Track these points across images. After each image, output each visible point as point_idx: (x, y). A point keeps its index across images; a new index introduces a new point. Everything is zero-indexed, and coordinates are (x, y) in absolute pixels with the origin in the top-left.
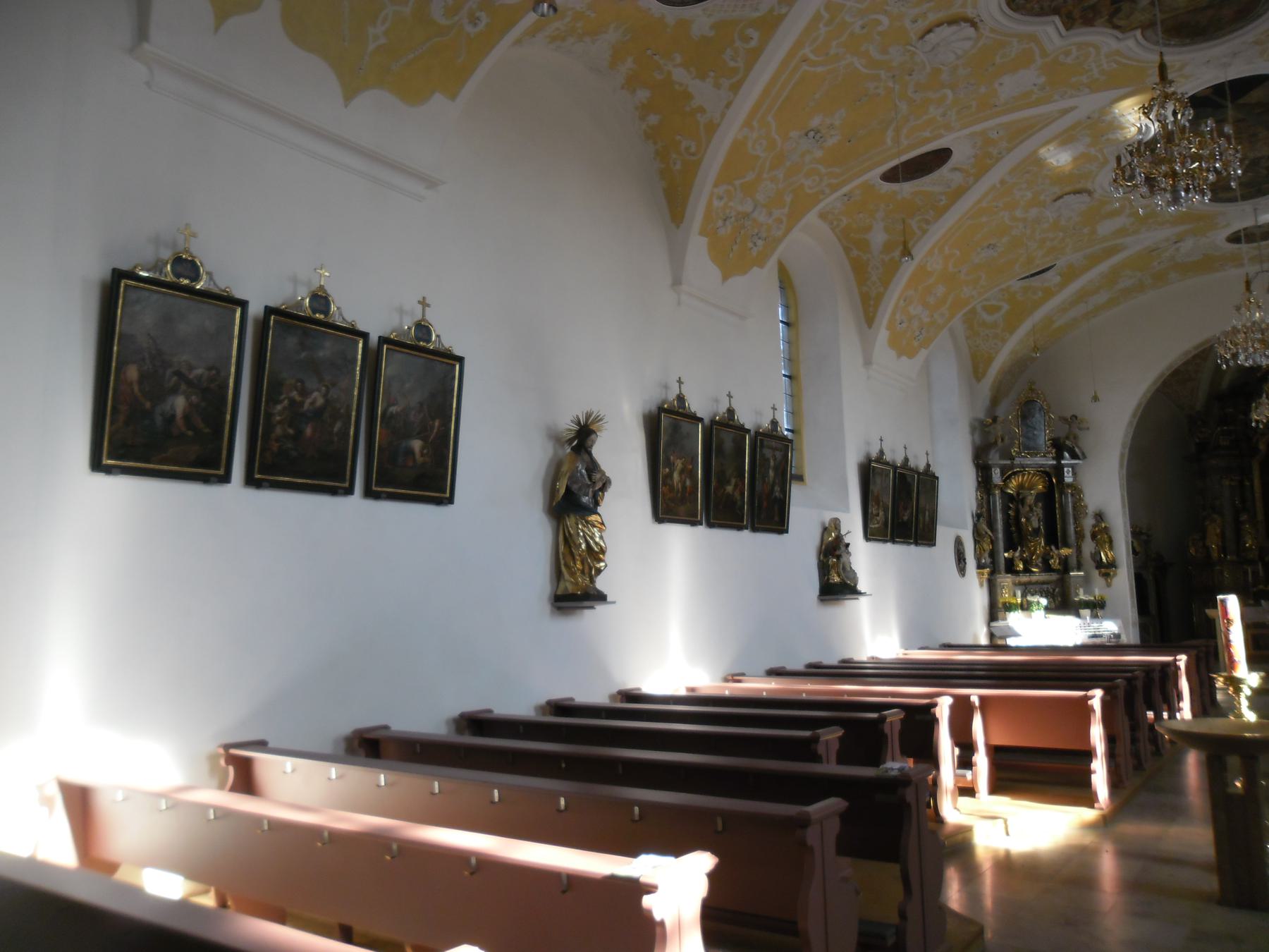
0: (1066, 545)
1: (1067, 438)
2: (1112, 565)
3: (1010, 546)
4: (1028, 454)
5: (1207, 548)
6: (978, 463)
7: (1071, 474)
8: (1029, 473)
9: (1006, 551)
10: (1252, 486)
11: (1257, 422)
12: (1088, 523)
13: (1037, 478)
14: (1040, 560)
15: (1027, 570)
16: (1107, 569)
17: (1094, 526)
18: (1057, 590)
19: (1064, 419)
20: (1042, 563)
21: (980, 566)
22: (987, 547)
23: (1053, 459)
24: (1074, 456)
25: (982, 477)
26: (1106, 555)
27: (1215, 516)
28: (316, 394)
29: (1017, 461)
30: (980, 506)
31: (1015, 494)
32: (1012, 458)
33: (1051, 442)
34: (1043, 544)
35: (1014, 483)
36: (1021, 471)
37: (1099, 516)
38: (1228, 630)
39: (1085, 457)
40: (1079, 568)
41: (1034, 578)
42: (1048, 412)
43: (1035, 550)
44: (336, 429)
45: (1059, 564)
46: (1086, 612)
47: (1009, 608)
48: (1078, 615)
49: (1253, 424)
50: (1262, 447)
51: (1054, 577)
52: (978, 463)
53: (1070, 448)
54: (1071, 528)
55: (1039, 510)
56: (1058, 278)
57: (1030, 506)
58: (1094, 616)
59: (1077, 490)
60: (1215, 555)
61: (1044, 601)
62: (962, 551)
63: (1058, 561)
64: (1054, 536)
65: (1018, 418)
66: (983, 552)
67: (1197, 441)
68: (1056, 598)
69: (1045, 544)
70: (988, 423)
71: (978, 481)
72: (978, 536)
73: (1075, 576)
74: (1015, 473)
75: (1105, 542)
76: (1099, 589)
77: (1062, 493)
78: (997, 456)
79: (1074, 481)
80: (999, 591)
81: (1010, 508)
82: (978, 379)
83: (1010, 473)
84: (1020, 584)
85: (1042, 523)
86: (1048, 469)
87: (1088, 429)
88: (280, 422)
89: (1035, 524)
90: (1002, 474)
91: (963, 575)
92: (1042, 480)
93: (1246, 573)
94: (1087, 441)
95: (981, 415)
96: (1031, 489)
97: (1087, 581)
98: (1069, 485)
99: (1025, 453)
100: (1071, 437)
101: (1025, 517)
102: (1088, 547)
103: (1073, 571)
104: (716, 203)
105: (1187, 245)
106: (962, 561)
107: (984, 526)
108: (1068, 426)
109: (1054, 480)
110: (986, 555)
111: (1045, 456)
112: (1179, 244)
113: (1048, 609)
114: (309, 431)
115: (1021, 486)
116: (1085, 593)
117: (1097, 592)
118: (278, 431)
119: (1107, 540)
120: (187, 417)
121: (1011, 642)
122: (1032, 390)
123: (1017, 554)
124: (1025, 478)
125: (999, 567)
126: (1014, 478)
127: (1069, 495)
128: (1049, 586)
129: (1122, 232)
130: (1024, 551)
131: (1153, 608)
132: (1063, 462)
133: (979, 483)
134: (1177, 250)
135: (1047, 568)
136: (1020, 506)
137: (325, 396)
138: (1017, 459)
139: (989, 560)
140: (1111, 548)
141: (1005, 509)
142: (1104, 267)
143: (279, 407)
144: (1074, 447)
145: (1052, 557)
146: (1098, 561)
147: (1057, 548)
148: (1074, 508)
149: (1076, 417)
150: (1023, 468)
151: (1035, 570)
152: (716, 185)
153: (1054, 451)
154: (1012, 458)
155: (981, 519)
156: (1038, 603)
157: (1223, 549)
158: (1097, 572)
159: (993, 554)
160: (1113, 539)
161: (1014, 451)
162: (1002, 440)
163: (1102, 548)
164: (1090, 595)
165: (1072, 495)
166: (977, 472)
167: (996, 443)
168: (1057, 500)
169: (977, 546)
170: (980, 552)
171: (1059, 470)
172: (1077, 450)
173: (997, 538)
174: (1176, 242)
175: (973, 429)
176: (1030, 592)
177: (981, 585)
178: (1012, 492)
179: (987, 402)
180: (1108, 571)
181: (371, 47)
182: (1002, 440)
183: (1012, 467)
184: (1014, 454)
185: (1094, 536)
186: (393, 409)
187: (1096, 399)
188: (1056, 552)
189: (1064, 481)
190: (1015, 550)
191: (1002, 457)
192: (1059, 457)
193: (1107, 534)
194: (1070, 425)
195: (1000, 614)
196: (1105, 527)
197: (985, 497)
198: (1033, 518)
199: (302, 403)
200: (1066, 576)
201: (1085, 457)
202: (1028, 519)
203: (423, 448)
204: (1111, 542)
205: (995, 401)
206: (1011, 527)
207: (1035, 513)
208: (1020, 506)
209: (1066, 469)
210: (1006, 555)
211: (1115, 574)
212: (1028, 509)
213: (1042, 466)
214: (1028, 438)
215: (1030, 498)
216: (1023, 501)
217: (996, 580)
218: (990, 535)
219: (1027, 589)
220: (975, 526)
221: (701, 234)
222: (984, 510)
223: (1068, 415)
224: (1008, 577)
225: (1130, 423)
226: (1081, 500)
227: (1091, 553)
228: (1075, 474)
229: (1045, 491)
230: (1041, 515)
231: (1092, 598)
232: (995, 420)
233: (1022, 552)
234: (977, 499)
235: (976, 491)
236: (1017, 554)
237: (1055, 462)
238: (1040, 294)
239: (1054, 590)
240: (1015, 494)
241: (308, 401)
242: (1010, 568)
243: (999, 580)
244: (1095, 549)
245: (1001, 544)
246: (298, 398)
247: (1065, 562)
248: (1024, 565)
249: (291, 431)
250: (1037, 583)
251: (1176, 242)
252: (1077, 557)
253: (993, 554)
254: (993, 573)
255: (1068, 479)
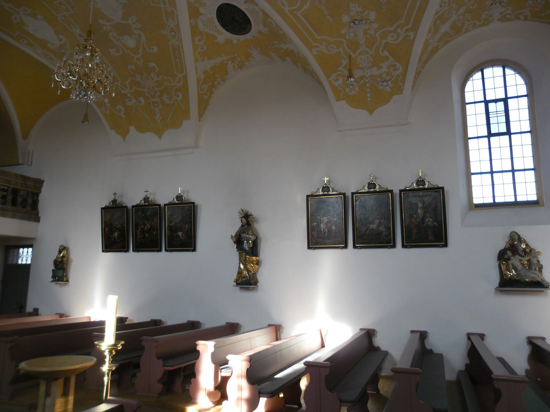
28: (148, 225)
44: (154, 233)
88: (139, 234)
104: (336, 84)
114: (147, 235)
118: (139, 237)
120: (118, 237)
137: (150, 225)
143: (139, 231)
152: (328, 77)
181: (159, 121)
186: (171, 224)
199: (144, 228)
203: (182, 235)
221: (338, 100)
241: (146, 227)
246: (143, 227)
249: (142, 236)
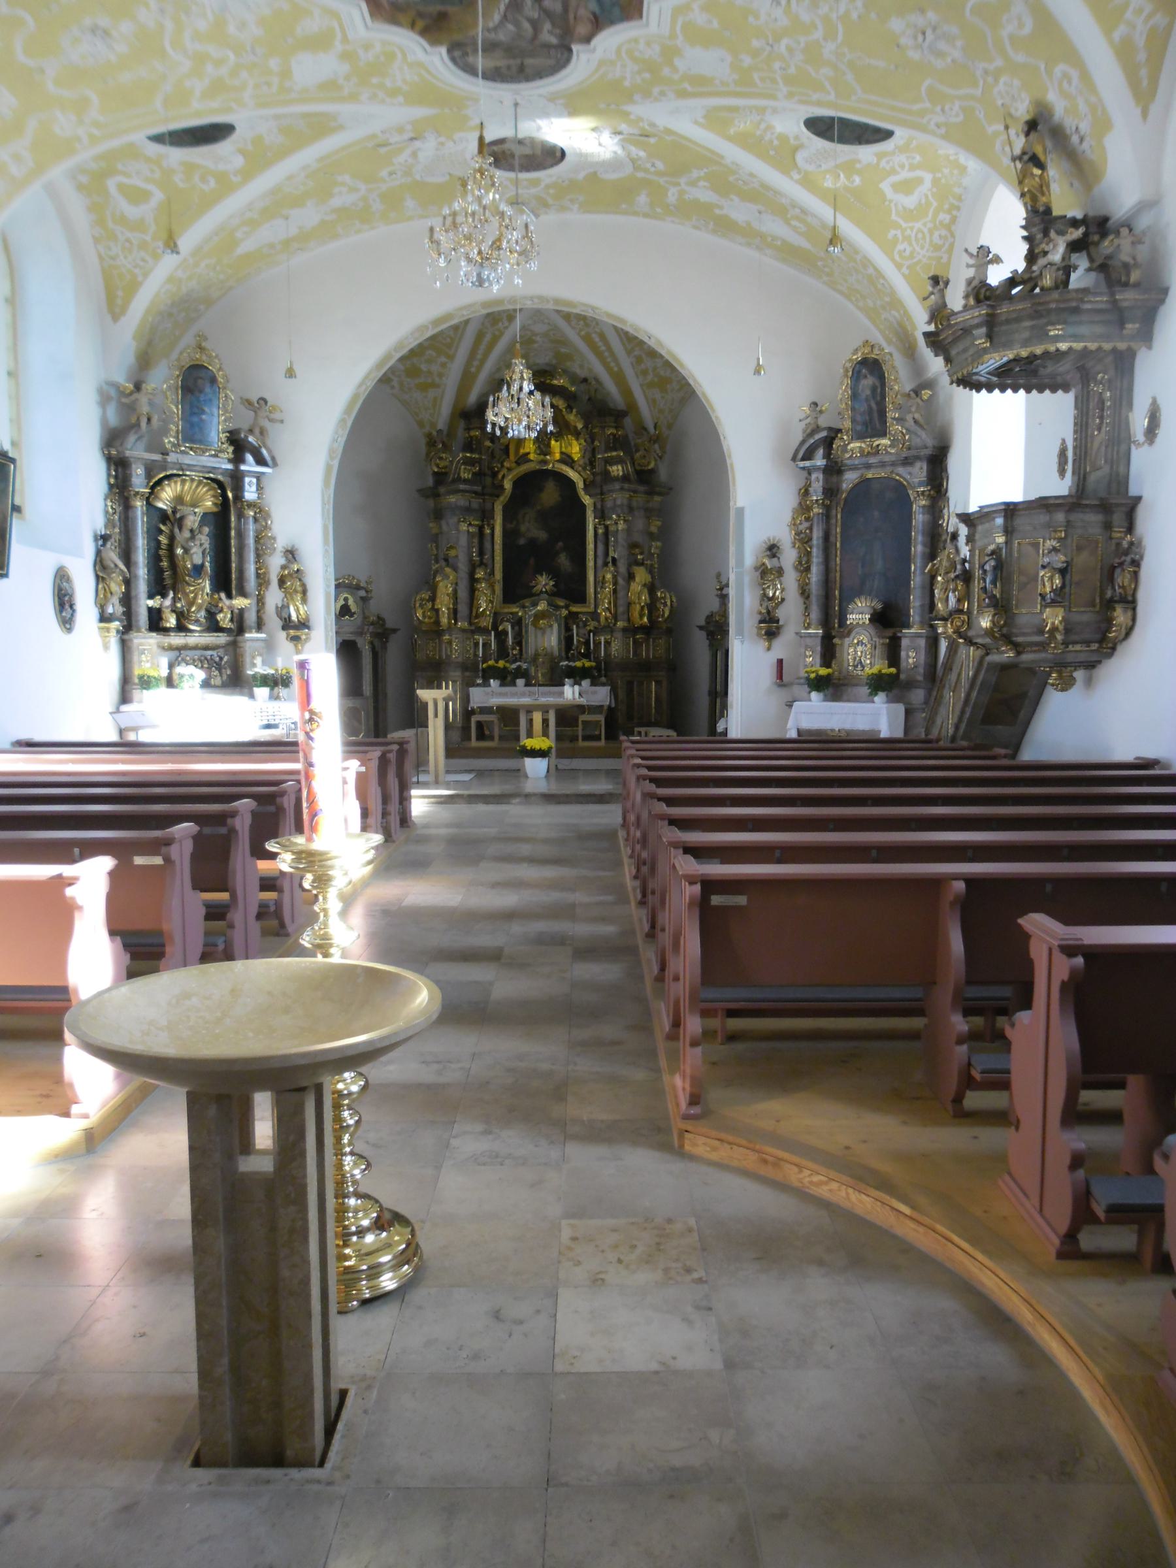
0: (243, 593)
1: (251, 431)
2: (304, 625)
3: (158, 588)
4: (191, 449)
5: (437, 611)
6: (109, 454)
7: (254, 488)
8: (192, 480)
9: (151, 597)
10: (493, 535)
11: (494, 425)
12: (275, 562)
13: (205, 489)
14: (203, 613)
15: (181, 628)
16: (296, 628)
17: (283, 567)
18: (226, 659)
19: (248, 403)
20: (205, 618)
21: (104, 618)
22: (118, 588)
23: (230, 461)
24: (261, 461)
25: (116, 477)
26: (297, 610)
27: (448, 570)
29: (172, 458)
30: (109, 523)
31: (170, 512)
32: (165, 453)
33: (228, 434)
34: (208, 589)
35: (167, 496)
36: (179, 475)
37: (291, 554)
38: (311, 739)
39: (275, 464)
40: (260, 626)
41: (192, 640)
42: (225, 388)
43: (195, 598)
45: (232, 620)
46: (262, 692)
47: (146, 683)
48: (252, 696)
49: (489, 427)
50: (508, 485)
51: (222, 639)
52: (109, 454)
53: (255, 447)
54: (251, 569)
55: (204, 539)
56: (239, 161)
57: (192, 531)
58: (274, 697)
59: (261, 513)
60: (444, 621)
61: (200, 675)
62: (69, 592)
63: (229, 616)
64: (224, 582)
65: (177, 389)
66: (109, 595)
67: (436, 470)
68: (224, 670)
69: (211, 590)
70: (128, 391)
71: (109, 484)
72: (101, 569)
73: (253, 640)
74: (168, 477)
75: (296, 591)
76: (285, 658)
77: (241, 516)
78: (141, 445)
79: (259, 498)
80: (135, 658)
81: (161, 532)
82: (115, 318)
83: (161, 476)
84: (171, 648)
85: (209, 559)
86: (220, 477)
87: (282, 421)
89: (198, 560)
90: (149, 474)
91: (69, 630)
92: (211, 493)
93: (476, 644)
94: (280, 441)
95: (121, 378)
96: (194, 505)
97: (269, 647)
98: (251, 505)
99: (186, 447)
100: (257, 431)
101: (183, 547)
102: (274, 597)
103: (250, 632)
105: (428, 148)
106: (67, 606)
107: (113, 556)
108: (252, 413)
109: (230, 495)
110: (115, 600)
111: (216, 456)
112: (417, 144)
113: (206, 684)
115: (179, 500)
116: (264, 663)
117: (280, 663)
119: (299, 589)
121: (144, 736)
122: (201, 348)
123: (168, 602)
124: (186, 487)
125: (137, 621)
126: (169, 485)
127: (251, 519)
128: (214, 653)
129: (329, 88)
130: (180, 599)
131: (367, 688)
132: (243, 467)
133: (111, 486)
134: (414, 154)
135: (213, 626)
136: (176, 530)
138: (171, 454)
139: (120, 610)
140: (304, 600)
141: (153, 533)
142: (309, 155)
144: (260, 447)
145: (221, 611)
146: (285, 619)
147: (229, 596)
148: (258, 539)
149: (266, 402)
150: (183, 470)
151: (192, 627)
153: (231, 449)
154: (165, 453)
155: (109, 544)
156: (191, 676)
157: (454, 613)
158: (283, 634)
159: (127, 600)
160: (309, 587)
161: (169, 441)
162: (149, 420)
163: (292, 599)
164: (270, 667)
165: (256, 520)
166: (109, 469)
167: (137, 425)
168: (233, 525)
169: (100, 586)
170: (105, 596)
171: (237, 479)
172: (264, 451)
173: (136, 577)
174: (412, 139)
175: (104, 400)
176: (184, 660)
177: (106, 647)
178: (165, 507)
179: (130, 359)
180: (298, 633)
182: (149, 420)
183: (164, 466)
184: (168, 446)
185: (282, 582)
187: (290, 373)
188: (227, 602)
189: (243, 497)
190: (164, 596)
191: (149, 449)
192: (238, 459)
193: (300, 580)
194: (255, 412)
195: (137, 694)
196: (298, 570)
197: (118, 510)
198: (194, 550)
200: (240, 638)
201: (275, 464)
202: (186, 551)
204: (304, 592)
205: (144, 362)
206: (161, 561)
207: (198, 543)
208: (176, 530)
209: (247, 480)
210: (150, 603)
211: (307, 639)
212: (187, 534)
213: (213, 469)
214: (192, 425)
215: (191, 518)
216: (180, 522)
217: (131, 640)
218: (121, 570)
219: (179, 654)
220: (98, 553)
222: (117, 530)
223: (254, 398)
224: (152, 637)
225: (342, 421)
226: (266, 527)
227: (277, 607)
228: (262, 488)
229: (215, 509)
230: (207, 545)
231: (273, 672)
232: (138, 387)
233: (174, 600)
234: (107, 512)
235: (105, 500)
236: (168, 602)
237: (230, 466)
238: (212, 183)
239: (221, 659)
240: (170, 512)
242: (155, 623)
243: (136, 641)
244: (283, 600)
245: (142, 587)
247: (239, 618)
248: (178, 620)
250: (196, 648)
251: (412, 139)
252: (258, 612)
253: (127, 600)
254: (129, 626)
255: (250, 494)
